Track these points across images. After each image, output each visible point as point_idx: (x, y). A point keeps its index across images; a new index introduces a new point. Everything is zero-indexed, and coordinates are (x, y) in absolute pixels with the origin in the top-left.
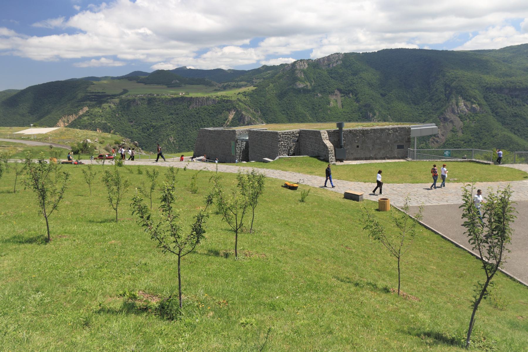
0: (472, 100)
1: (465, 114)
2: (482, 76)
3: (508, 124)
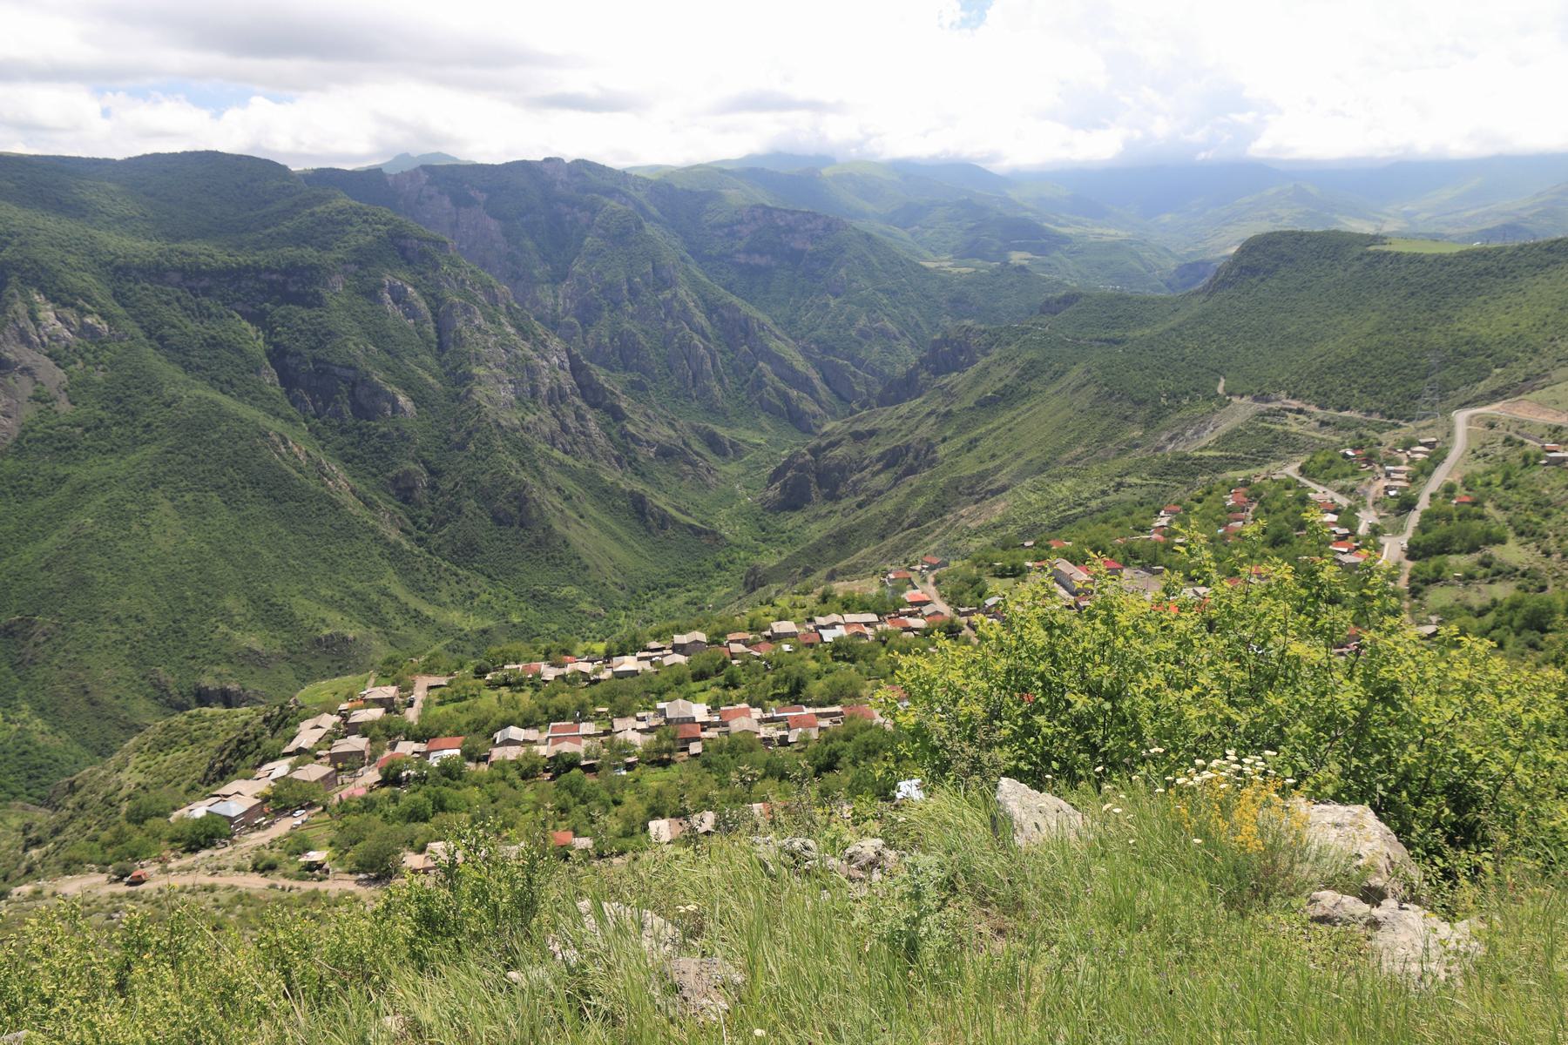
0: (80, 302)
1: (67, 347)
2: (92, 232)
3: (198, 368)
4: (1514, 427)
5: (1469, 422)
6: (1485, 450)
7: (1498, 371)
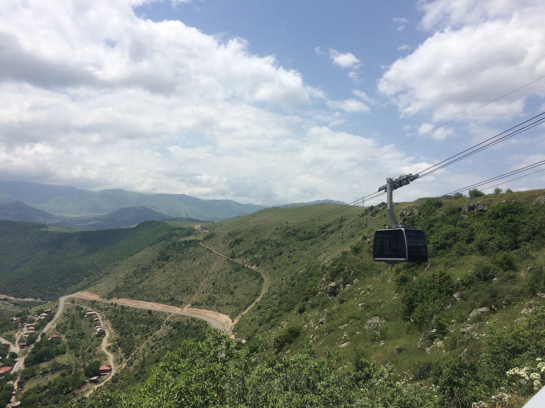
4: (81, 302)
5: (66, 301)
6: (69, 313)
7: (85, 278)
